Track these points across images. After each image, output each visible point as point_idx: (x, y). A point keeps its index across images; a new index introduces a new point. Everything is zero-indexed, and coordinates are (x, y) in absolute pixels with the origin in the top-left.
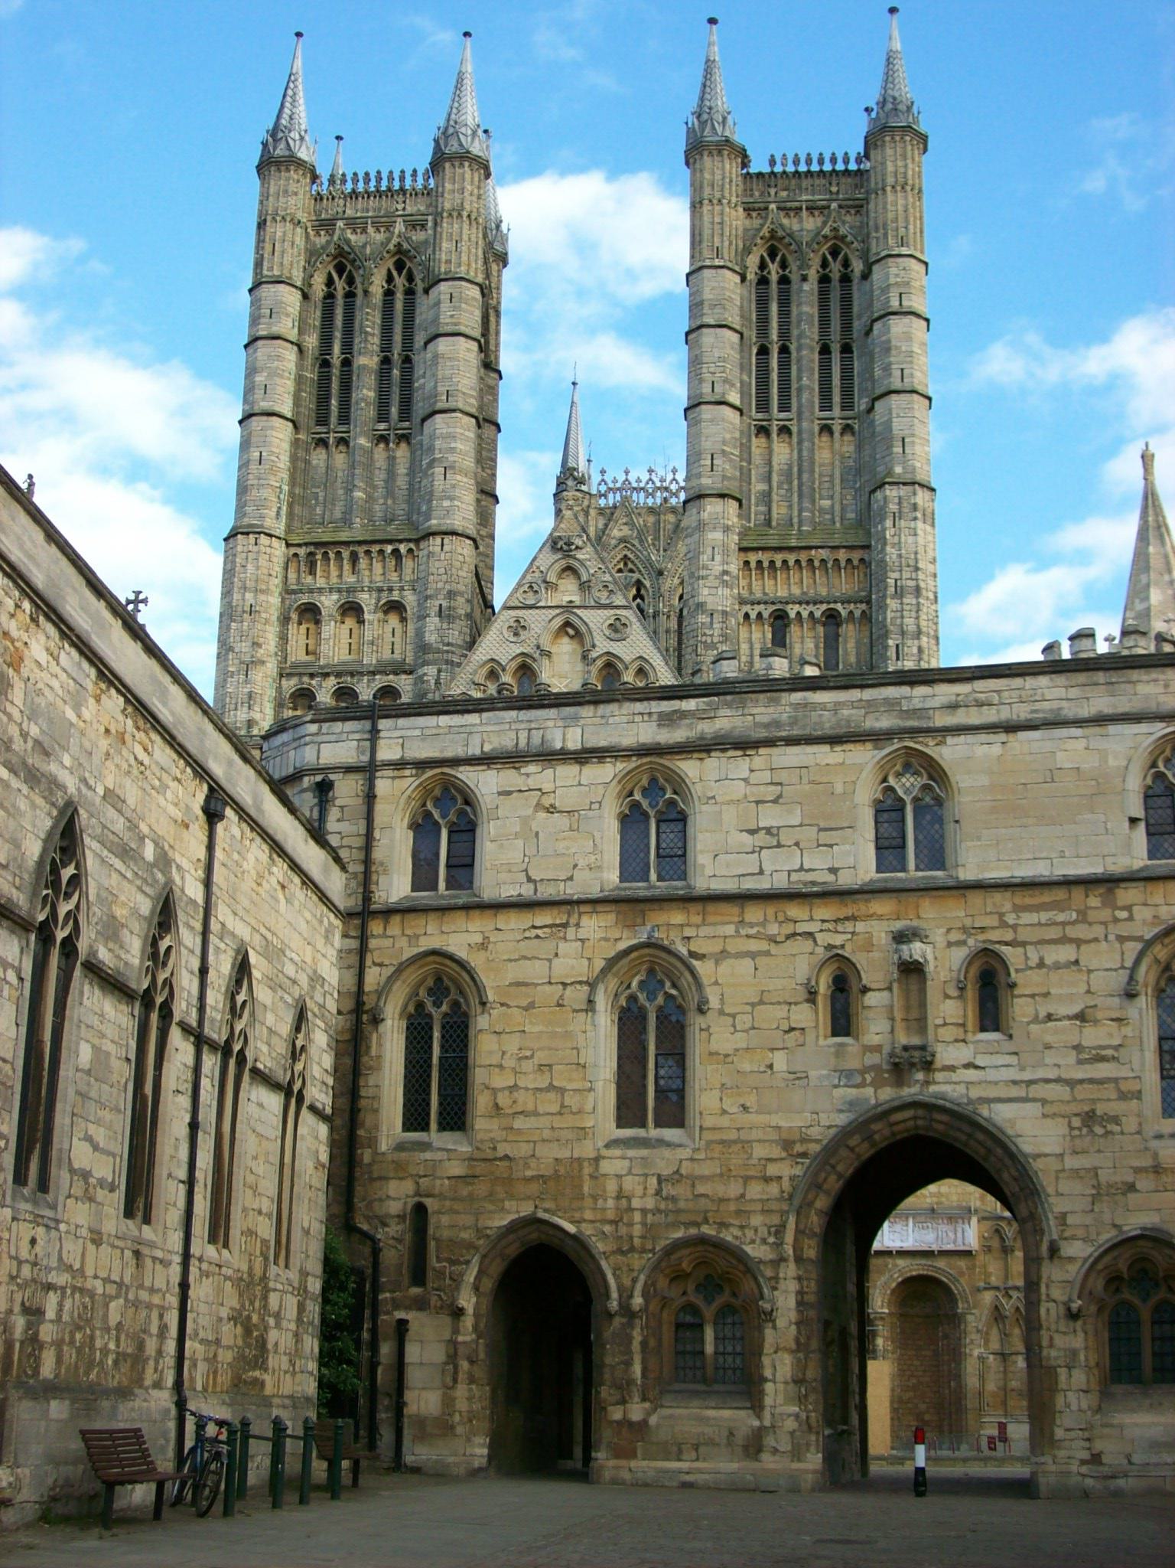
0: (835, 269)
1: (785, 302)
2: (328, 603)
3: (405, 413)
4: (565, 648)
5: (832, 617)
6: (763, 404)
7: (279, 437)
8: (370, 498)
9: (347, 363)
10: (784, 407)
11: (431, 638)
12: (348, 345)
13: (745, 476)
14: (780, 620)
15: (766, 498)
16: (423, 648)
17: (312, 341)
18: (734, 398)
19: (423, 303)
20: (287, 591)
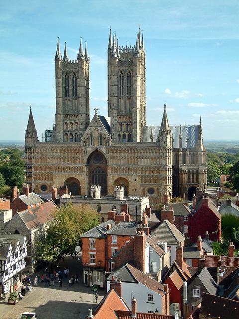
0: (129, 75)
1: (123, 78)
2: (68, 122)
3: (76, 95)
4: (96, 131)
5: (128, 124)
6: (120, 95)
7: (61, 100)
8: (73, 107)
9: (68, 88)
10: (123, 95)
11: (81, 127)
12: (68, 86)
13: (118, 105)
14: (122, 125)
15: (120, 107)
16: (80, 128)
17: (64, 85)
18: (116, 95)
19: (78, 80)
20: (63, 121)
